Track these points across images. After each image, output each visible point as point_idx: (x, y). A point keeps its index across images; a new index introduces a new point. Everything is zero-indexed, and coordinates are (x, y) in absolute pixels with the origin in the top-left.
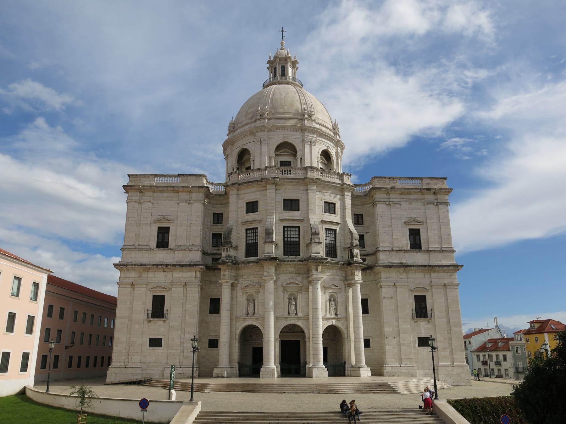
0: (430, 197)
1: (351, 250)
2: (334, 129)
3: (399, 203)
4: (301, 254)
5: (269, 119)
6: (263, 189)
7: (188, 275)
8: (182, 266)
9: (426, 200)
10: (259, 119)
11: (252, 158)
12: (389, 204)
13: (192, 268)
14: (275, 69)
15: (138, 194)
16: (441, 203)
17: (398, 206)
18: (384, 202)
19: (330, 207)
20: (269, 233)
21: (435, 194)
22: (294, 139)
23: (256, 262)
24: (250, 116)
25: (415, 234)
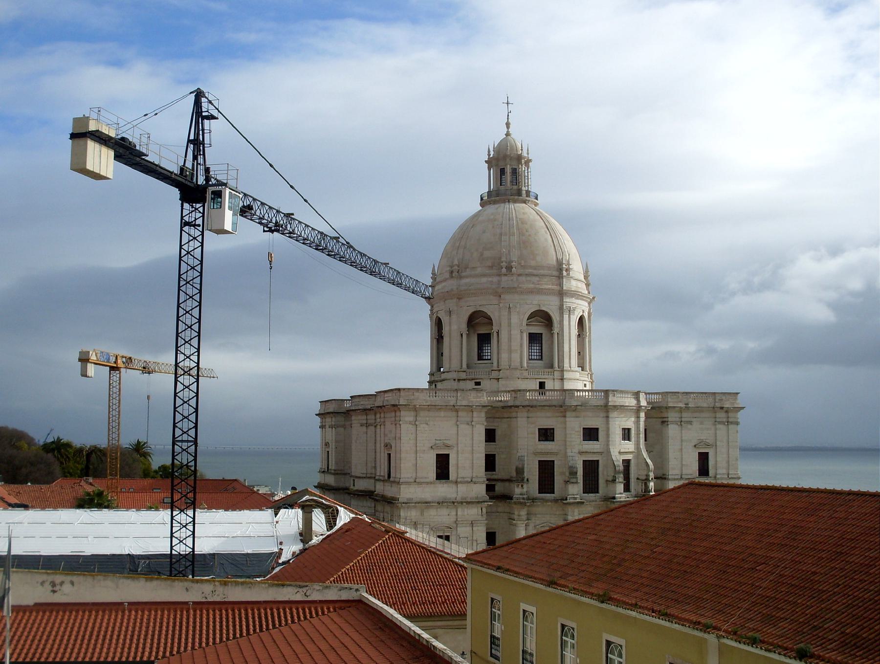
0: (721, 415)
1: (646, 484)
2: (586, 277)
3: (690, 423)
4: (600, 491)
5: (519, 275)
6: (561, 414)
7: (473, 512)
8: (468, 503)
9: (718, 420)
10: (505, 275)
11: (495, 328)
12: (681, 423)
13: (479, 505)
14: (502, 172)
15: (413, 413)
16: (732, 423)
17: (689, 426)
18: (675, 423)
19: (626, 434)
20: (573, 473)
21: (727, 412)
22: (550, 305)
23: (556, 501)
24: (489, 263)
25: (703, 458)
